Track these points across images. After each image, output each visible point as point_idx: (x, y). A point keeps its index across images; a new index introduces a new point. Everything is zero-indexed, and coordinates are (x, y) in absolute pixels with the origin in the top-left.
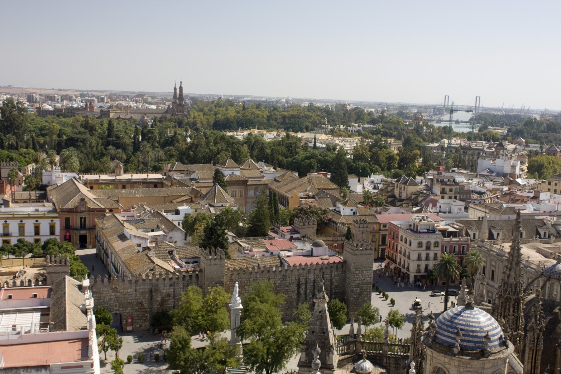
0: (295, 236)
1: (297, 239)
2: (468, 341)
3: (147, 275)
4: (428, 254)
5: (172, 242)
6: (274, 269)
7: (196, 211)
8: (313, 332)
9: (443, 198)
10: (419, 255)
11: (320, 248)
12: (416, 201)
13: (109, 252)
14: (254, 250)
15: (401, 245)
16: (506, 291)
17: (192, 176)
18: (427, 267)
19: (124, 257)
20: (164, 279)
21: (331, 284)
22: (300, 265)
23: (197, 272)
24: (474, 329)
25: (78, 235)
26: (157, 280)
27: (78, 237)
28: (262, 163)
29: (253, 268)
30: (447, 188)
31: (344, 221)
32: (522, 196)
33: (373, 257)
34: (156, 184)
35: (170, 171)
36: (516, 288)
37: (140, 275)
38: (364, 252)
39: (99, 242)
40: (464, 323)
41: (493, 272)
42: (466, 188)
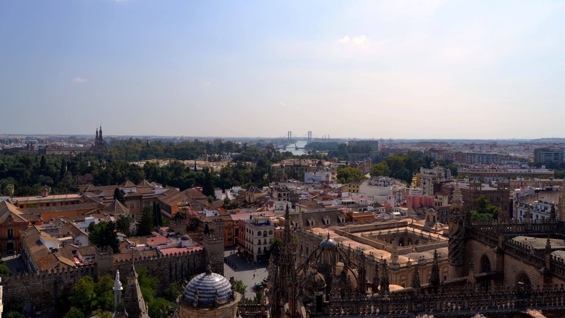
0: (171, 234)
2: (204, 297)
3: (52, 270)
4: (265, 240)
5: (76, 245)
6: (152, 259)
7: (99, 220)
8: (127, 302)
9: (279, 200)
10: (259, 241)
11: (186, 241)
12: (258, 204)
13: (28, 255)
14: (137, 246)
15: (248, 235)
16: (282, 260)
17: (101, 195)
18: (265, 248)
20: (66, 273)
21: (195, 266)
22: (171, 254)
23: (92, 266)
24: (208, 288)
26: (61, 274)
27: (6, 246)
28: (154, 183)
29: (136, 259)
30: (282, 193)
32: (331, 196)
33: (223, 244)
35: (85, 191)
36: (289, 258)
37: (47, 271)
38: (216, 242)
39: (22, 248)
41: (307, 248)
42: (295, 193)
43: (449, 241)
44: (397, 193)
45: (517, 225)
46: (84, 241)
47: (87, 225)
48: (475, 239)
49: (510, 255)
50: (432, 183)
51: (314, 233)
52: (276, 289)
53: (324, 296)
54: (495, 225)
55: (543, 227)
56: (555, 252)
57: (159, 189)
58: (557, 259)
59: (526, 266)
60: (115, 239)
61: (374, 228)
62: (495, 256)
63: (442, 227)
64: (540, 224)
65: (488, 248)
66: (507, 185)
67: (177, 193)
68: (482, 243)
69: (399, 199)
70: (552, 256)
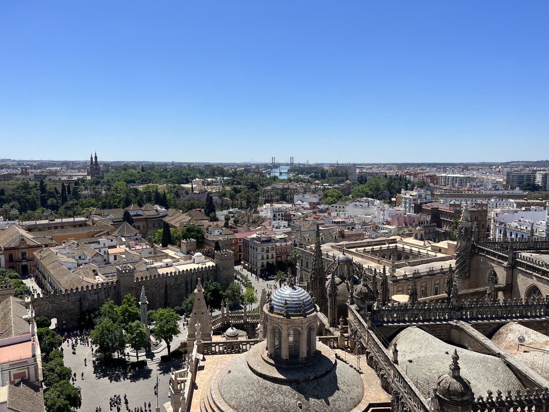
4: (268, 255)
9: (274, 220)
10: (263, 256)
13: (46, 275)
16: (314, 274)
18: (268, 262)
22: (187, 270)
24: (295, 299)
25: (20, 266)
31: (215, 239)
34: (82, 225)
61: (366, 244)
63: (430, 243)
66: (486, 205)
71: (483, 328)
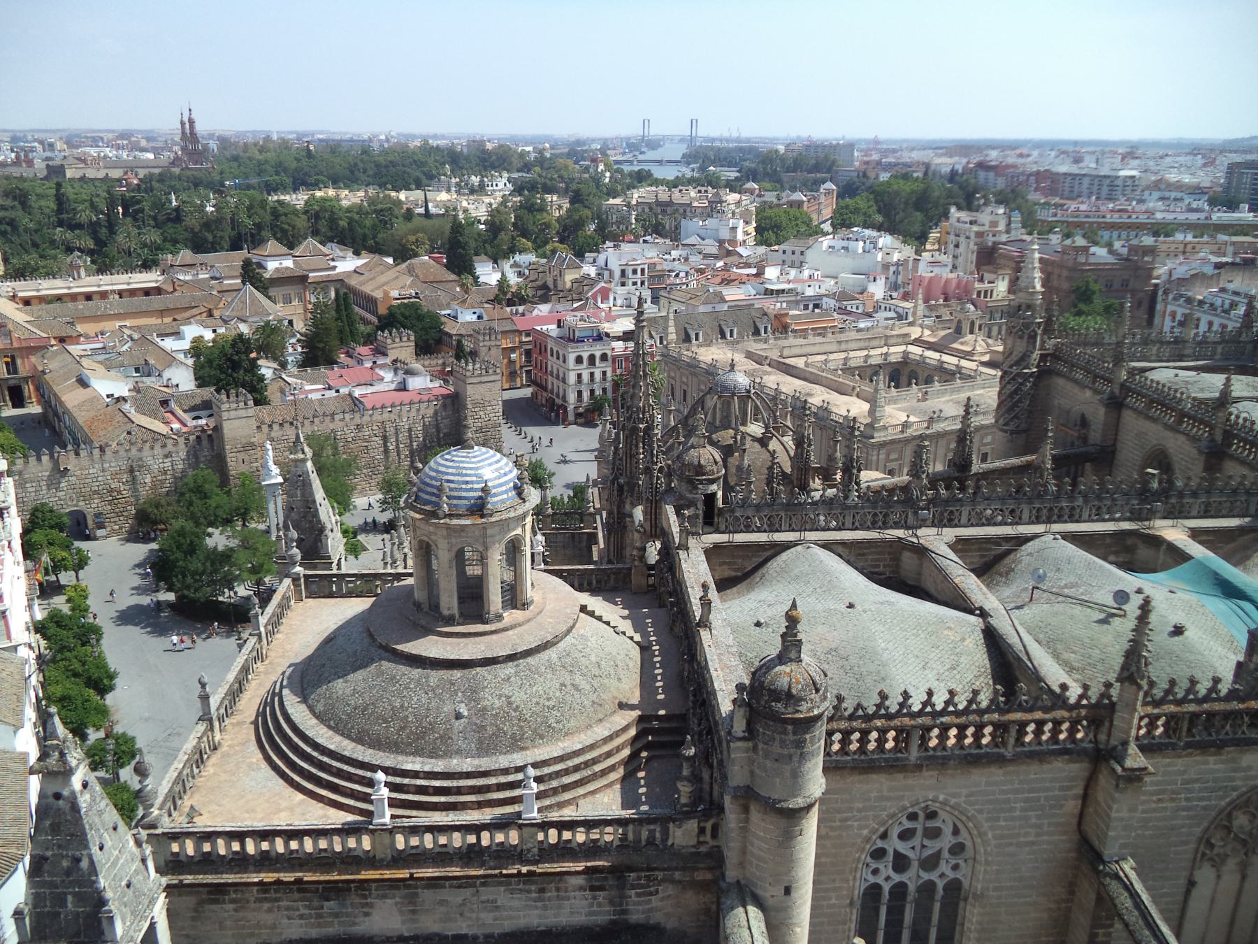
1: (383, 366)
4: (592, 374)
7: (214, 331)
9: (623, 284)
10: (579, 376)
15: (552, 363)
19: (82, 417)
21: (438, 432)
24: (468, 479)
28: (334, 245)
32: (741, 275)
40: (454, 471)
43: (1002, 377)
44: (892, 269)
45: (1162, 343)
46: (183, 378)
47: (186, 344)
48: (1059, 374)
49: (1135, 410)
50: (976, 244)
51: (701, 358)
52: (616, 478)
53: (720, 494)
54: (1110, 344)
55: (1219, 349)
56: (1147, 374)
57: (347, 264)
58: (1241, 421)
59: (1169, 434)
60: (254, 375)
62: (1102, 411)
64: (1215, 343)
65: (1088, 393)
66: (1151, 251)
67: (389, 267)
68: (1076, 381)
69: (896, 283)
70: (1231, 414)
71: (980, 550)
